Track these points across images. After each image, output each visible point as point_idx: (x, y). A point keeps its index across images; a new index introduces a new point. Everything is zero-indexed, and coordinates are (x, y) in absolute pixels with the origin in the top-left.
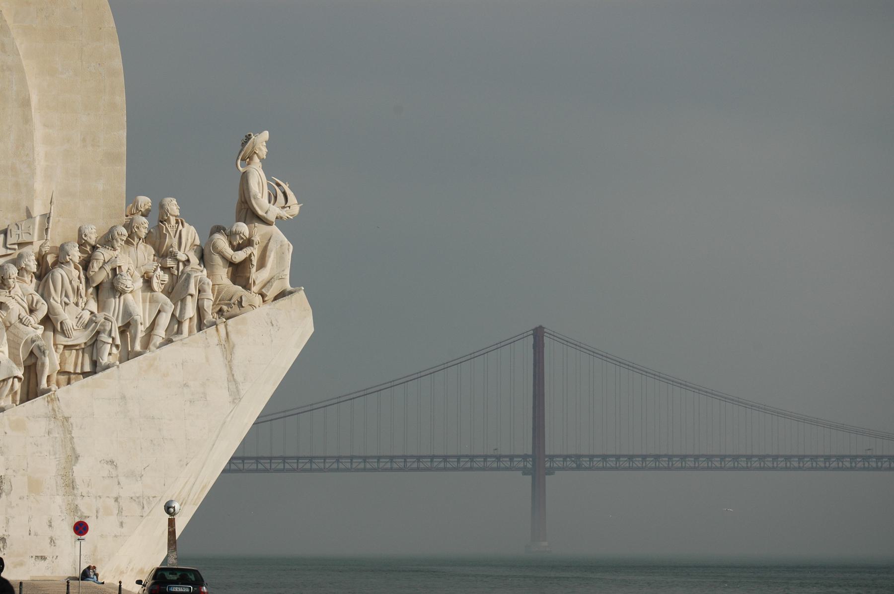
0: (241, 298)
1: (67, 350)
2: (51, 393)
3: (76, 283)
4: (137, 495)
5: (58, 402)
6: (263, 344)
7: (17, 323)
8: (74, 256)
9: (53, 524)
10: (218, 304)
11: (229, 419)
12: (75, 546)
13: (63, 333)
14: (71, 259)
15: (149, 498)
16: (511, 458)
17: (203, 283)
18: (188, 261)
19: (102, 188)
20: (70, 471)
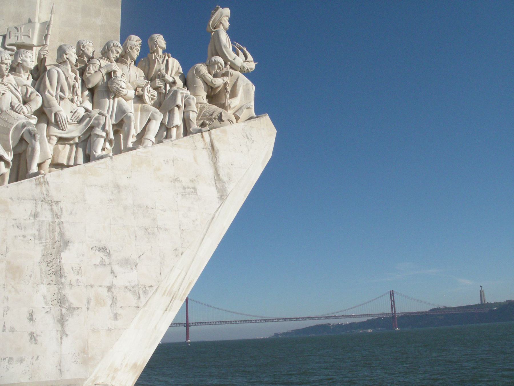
0: (221, 114)
1: (60, 144)
2: (40, 176)
3: (72, 81)
4: (133, 284)
5: (47, 185)
6: (242, 152)
7: (9, 109)
8: (71, 55)
9: (34, 317)
10: (201, 119)
11: (217, 215)
12: (61, 343)
13: (57, 125)
14: (67, 59)
15: (145, 288)
16: (182, 324)
17: (188, 98)
18: (174, 83)
19: (100, 24)
20: (58, 257)
